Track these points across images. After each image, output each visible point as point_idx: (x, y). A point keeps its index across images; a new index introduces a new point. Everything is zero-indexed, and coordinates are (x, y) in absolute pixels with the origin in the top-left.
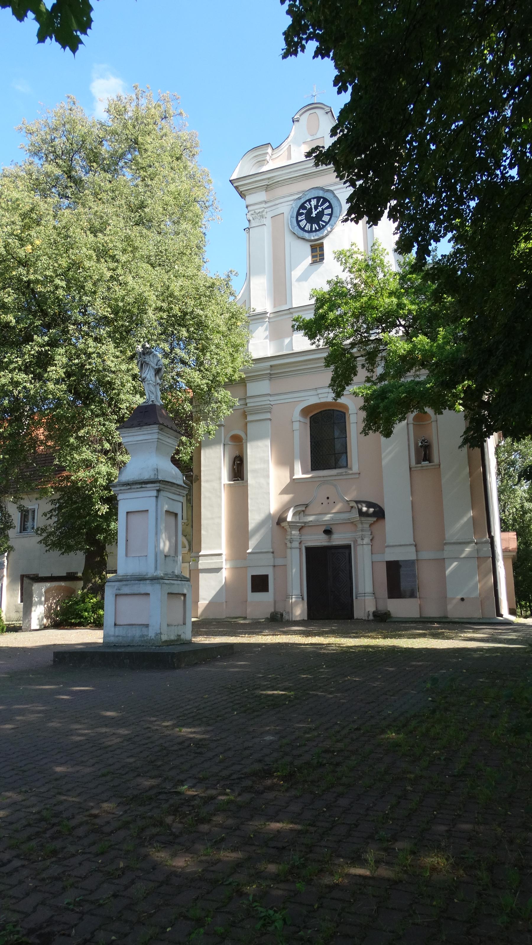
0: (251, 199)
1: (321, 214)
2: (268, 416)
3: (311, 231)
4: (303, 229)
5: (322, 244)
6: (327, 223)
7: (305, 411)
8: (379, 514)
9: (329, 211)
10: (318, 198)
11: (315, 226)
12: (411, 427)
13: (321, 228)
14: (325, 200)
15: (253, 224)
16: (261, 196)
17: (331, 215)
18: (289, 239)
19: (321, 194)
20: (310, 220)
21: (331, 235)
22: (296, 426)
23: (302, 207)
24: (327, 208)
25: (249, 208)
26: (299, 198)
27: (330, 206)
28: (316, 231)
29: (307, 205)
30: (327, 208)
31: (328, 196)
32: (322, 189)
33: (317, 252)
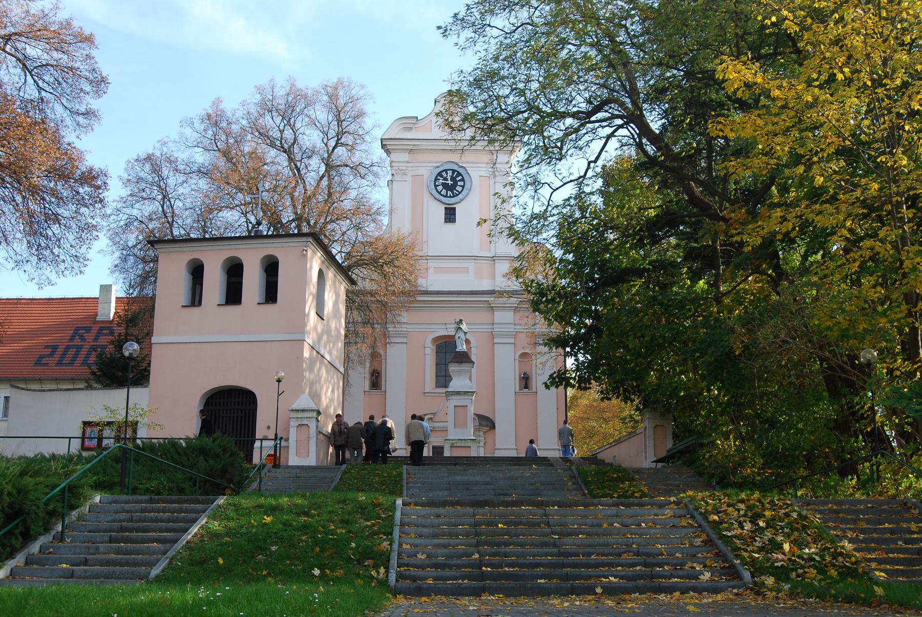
0: (395, 156)
1: (455, 184)
2: (404, 340)
3: (446, 196)
4: (440, 193)
5: (454, 209)
6: (460, 193)
7: (435, 340)
8: (492, 425)
9: (461, 183)
10: (454, 171)
11: (449, 193)
12: (517, 362)
13: (454, 196)
14: (459, 174)
15: (397, 178)
16: (405, 156)
17: (463, 187)
18: (427, 198)
19: (456, 168)
20: (445, 186)
21: (462, 203)
22: (428, 351)
23: (440, 174)
24: (460, 180)
25: (393, 164)
26: (438, 167)
27: (463, 180)
28: (450, 197)
29: (444, 174)
30: (460, 180)
31: (460, 170)
32: (457, 164)
33: (450, 215)
